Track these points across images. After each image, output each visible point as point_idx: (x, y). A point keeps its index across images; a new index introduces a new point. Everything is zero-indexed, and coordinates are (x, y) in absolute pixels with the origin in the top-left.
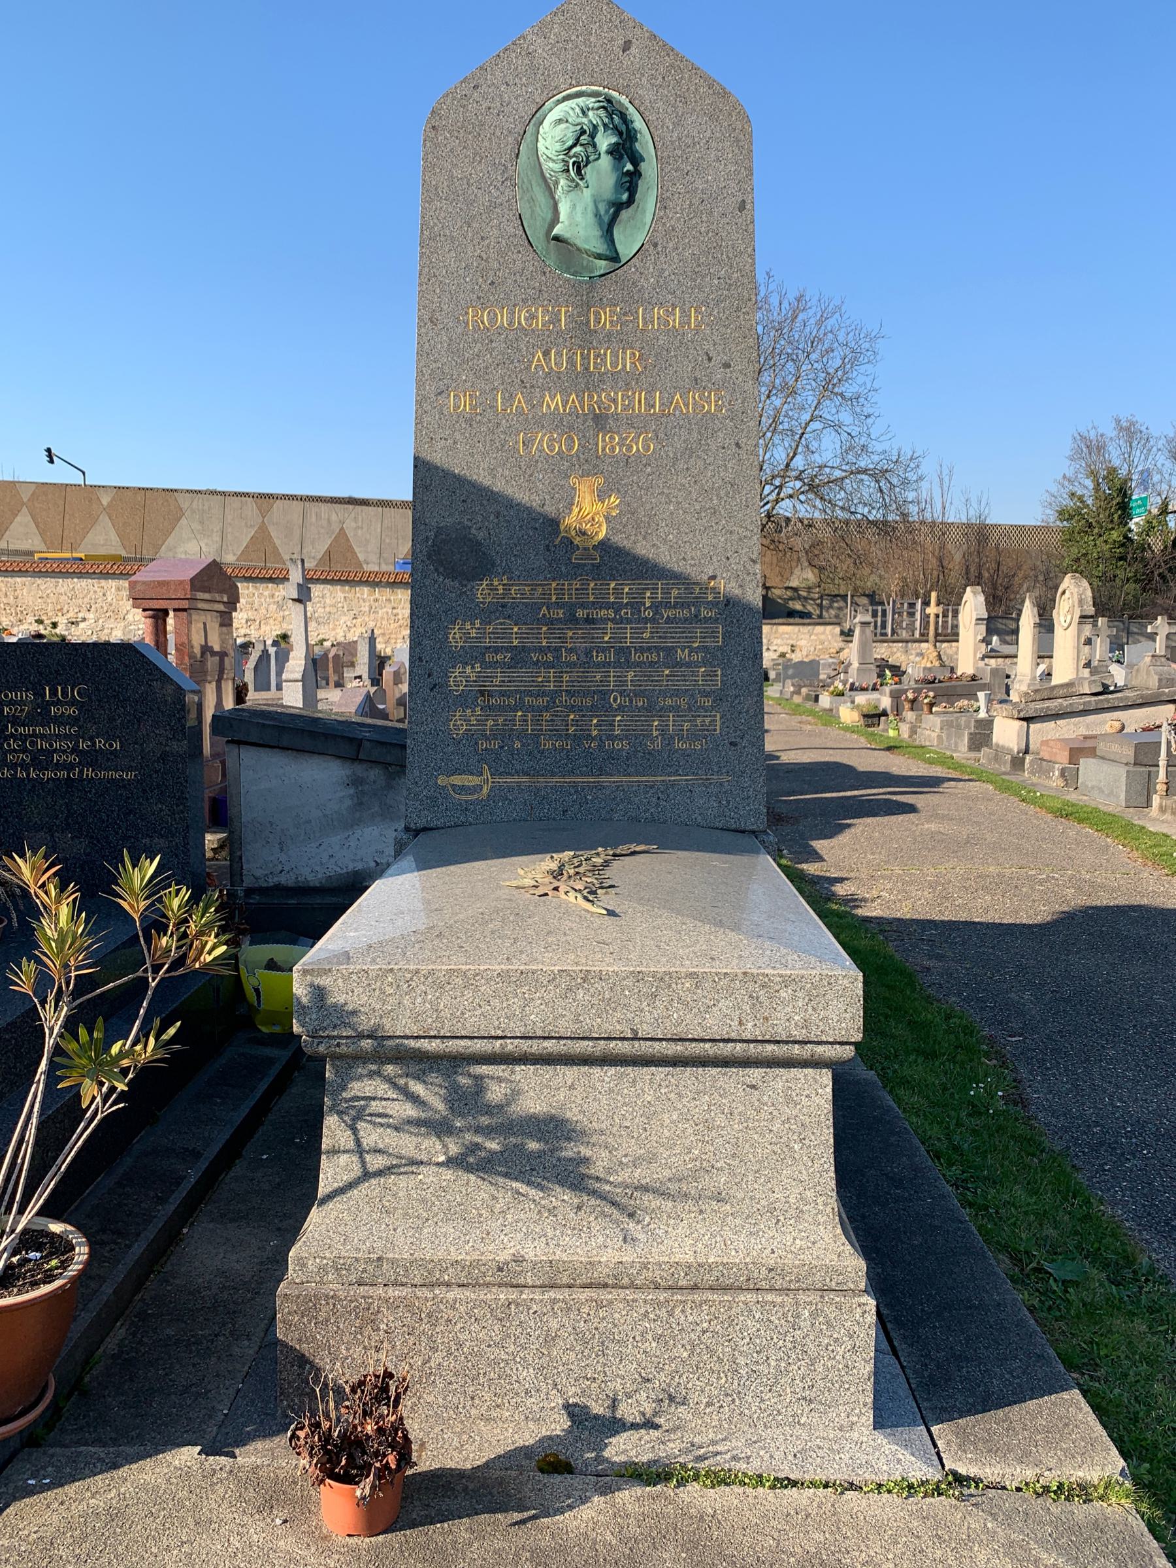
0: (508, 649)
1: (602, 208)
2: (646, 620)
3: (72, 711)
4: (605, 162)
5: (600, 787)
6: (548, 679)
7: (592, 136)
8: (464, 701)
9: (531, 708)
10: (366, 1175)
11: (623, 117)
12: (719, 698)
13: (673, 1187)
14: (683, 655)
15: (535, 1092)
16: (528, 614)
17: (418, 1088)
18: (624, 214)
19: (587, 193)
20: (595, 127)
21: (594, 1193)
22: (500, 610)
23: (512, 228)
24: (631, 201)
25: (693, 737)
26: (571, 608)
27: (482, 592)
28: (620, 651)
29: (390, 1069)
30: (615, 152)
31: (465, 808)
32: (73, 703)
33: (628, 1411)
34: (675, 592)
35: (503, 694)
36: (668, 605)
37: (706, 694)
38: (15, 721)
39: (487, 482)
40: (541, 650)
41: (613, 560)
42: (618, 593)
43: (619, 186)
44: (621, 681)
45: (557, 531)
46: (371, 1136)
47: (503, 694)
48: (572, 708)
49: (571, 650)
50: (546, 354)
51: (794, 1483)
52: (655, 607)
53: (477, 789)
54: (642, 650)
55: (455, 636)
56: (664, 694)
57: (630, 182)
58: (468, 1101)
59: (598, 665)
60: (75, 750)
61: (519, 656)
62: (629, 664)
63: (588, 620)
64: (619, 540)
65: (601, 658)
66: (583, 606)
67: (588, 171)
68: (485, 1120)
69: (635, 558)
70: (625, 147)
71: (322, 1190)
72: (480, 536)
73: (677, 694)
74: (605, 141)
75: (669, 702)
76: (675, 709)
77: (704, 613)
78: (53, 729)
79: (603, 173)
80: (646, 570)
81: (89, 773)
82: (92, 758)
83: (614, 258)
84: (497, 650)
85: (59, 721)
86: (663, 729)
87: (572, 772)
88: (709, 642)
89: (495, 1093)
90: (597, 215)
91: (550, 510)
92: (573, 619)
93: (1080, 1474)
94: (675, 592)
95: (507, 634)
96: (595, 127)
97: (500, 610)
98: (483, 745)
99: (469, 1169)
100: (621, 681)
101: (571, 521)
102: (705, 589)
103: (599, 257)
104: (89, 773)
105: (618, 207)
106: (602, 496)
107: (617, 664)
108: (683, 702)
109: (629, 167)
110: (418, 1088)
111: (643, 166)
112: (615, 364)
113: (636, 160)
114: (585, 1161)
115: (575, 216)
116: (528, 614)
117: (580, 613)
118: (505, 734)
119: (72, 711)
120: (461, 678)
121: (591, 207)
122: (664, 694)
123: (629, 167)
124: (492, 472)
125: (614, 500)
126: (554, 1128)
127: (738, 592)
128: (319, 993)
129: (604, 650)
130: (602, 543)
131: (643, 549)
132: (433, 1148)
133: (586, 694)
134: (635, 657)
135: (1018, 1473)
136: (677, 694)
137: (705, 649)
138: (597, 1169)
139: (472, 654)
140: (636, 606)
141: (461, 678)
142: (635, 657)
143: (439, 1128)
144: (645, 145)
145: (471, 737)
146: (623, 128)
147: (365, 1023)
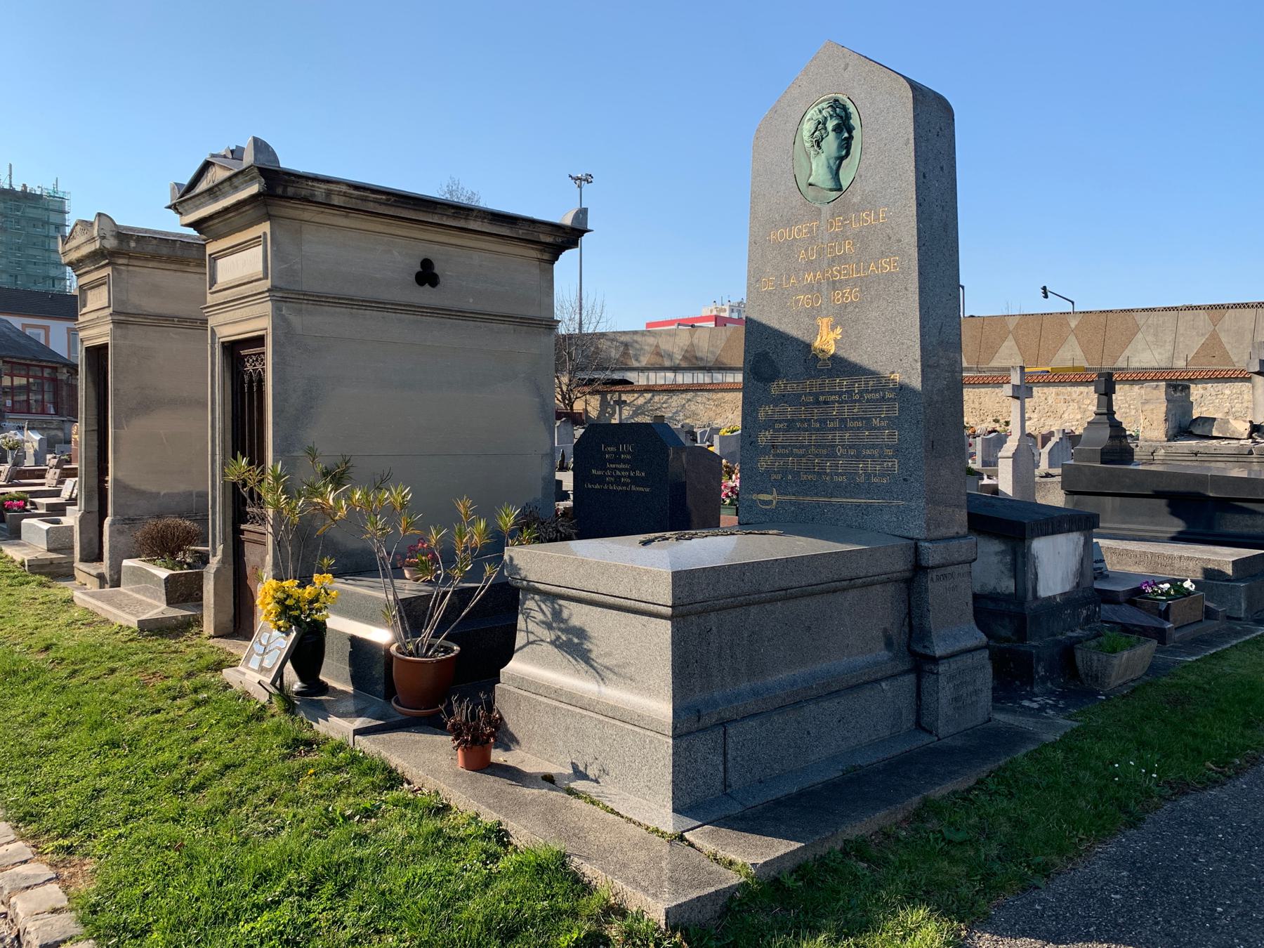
0: (786, 421)
1: (832, 162)
2: (856, 401)
3: (629, 457)
4: (832, 135)
5: (830, 504)
6: (805, 438)
7: (824, 124)
8: (764, 451)
9: (797, 456)
10: (529, 643)
11: (844, 108)
12: (897, 450)
13: (616, 670)
14: (876, 422)
15: (578, 615)
16: (793, 400)
17: (543, 606)
18: (844, 162)
19: (823, 156)
20: (826, 118)
21: (592, 666)
22: (783, 398)
23: (792, 184)
24: (848, 154)
25: (882, 476)
26: (816, 395)
27: (775, 389)
28: (843, 421)
29: (537, 597)
30: (838, 129)
31: (765, 512)
32: (629, 453)
33: (590, 773)
34: (871, 383)
35: (783, 447)
36: (867, 391)
37: (889, 447)
38: (611, 462)
39: (777, 327)
40: (802, 421)
41: (839, 366)
42: (840, 385)
43: (840, 147)
44: (842, 439)
45: (810, 351)
46: (532, 626)
47: (783, 447)
48: (817, 456)
49: (816, 421)
50: (806, 250)
51: (618, 814)
52: (861, 392)
53: (770, 502)
54: (853, 419)
55: (761, 415)
56: (865, 447)
57: (846, 145)
58: (557, 614)
59: (831, 429)
60: (629, 477)
61: (791, 425)
62: (847, 429)
63: (826, 402)
64: (842, 353)
65: (832, 425)
66: (822, 394)
67: (823, 144)
68: (562, 625)
69: (850, 363)
70: (844, 126)
71: (517, 647)
72: (774, 357)
73: (873, 447)
74: (831, 124)
75: (868, 452)
76: (872, 456)
77: (888, 395)
78: (622, 466)
79: (831, 143)
80: (855, 370)
81: (634, 488)
82: (635, 481)
83: (839, 188)
84: (780, 422)
85: (624, 461)
86: (865, 469)
87: (816, 495)
88: (891, 414)
89: (565, 614)
90: (829, 167)
91: (807, 339)
92: (817, 402)
93: (732, 857)
94: (871, 383)
95: (785, 412)
96: (826, 118)
97: (783, 398)
98: (774, 477)
99: (556, 647)
100: (842, 439)
101: (817, 344)
102: (888, 380)
103: (831, 190)
104: (634, 488)
105: (841, 159)
106: (833, 328)
107: (840, 429)
108: (876, 452)
109: (846, 135)
110: (543, 606)
111: (854, 133)
112: (840, 250)
113: (850, 130)
114: (590, 651)
115: (819, 170)
116: (793, 400)
117: (821, 398)
118: (784, 472)
119: (629, 457)
120: (764, 437)
121: (825, 163)
122: (865, 447)
123: (846, 135)
124: (780, 320)
125: (839, 330)
126: (581, 633)
127: (907, 381)
128: (511, 559)
129: (833, 420)
130: (833, 356)
131: (853, 357)
132: (548, 635)
133: (823, 447)
134: (849, 424)
135: (709, 847)
136: (873, 447)
137: (888, 418)
138: (593, 656)
139: (769, 424)
140: (850, 393)
141: (764, 437)
142: (849, 424)
143: (549, 627)
144: (855, 121)
145: (768, 472)
146: (843, 114)
147: (523, 574)
